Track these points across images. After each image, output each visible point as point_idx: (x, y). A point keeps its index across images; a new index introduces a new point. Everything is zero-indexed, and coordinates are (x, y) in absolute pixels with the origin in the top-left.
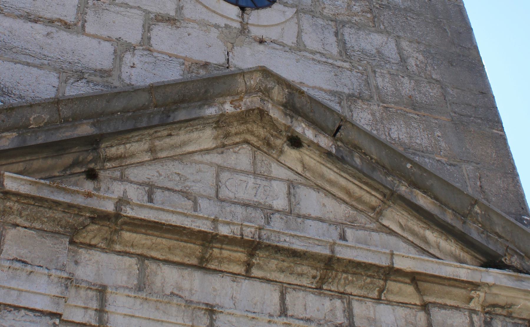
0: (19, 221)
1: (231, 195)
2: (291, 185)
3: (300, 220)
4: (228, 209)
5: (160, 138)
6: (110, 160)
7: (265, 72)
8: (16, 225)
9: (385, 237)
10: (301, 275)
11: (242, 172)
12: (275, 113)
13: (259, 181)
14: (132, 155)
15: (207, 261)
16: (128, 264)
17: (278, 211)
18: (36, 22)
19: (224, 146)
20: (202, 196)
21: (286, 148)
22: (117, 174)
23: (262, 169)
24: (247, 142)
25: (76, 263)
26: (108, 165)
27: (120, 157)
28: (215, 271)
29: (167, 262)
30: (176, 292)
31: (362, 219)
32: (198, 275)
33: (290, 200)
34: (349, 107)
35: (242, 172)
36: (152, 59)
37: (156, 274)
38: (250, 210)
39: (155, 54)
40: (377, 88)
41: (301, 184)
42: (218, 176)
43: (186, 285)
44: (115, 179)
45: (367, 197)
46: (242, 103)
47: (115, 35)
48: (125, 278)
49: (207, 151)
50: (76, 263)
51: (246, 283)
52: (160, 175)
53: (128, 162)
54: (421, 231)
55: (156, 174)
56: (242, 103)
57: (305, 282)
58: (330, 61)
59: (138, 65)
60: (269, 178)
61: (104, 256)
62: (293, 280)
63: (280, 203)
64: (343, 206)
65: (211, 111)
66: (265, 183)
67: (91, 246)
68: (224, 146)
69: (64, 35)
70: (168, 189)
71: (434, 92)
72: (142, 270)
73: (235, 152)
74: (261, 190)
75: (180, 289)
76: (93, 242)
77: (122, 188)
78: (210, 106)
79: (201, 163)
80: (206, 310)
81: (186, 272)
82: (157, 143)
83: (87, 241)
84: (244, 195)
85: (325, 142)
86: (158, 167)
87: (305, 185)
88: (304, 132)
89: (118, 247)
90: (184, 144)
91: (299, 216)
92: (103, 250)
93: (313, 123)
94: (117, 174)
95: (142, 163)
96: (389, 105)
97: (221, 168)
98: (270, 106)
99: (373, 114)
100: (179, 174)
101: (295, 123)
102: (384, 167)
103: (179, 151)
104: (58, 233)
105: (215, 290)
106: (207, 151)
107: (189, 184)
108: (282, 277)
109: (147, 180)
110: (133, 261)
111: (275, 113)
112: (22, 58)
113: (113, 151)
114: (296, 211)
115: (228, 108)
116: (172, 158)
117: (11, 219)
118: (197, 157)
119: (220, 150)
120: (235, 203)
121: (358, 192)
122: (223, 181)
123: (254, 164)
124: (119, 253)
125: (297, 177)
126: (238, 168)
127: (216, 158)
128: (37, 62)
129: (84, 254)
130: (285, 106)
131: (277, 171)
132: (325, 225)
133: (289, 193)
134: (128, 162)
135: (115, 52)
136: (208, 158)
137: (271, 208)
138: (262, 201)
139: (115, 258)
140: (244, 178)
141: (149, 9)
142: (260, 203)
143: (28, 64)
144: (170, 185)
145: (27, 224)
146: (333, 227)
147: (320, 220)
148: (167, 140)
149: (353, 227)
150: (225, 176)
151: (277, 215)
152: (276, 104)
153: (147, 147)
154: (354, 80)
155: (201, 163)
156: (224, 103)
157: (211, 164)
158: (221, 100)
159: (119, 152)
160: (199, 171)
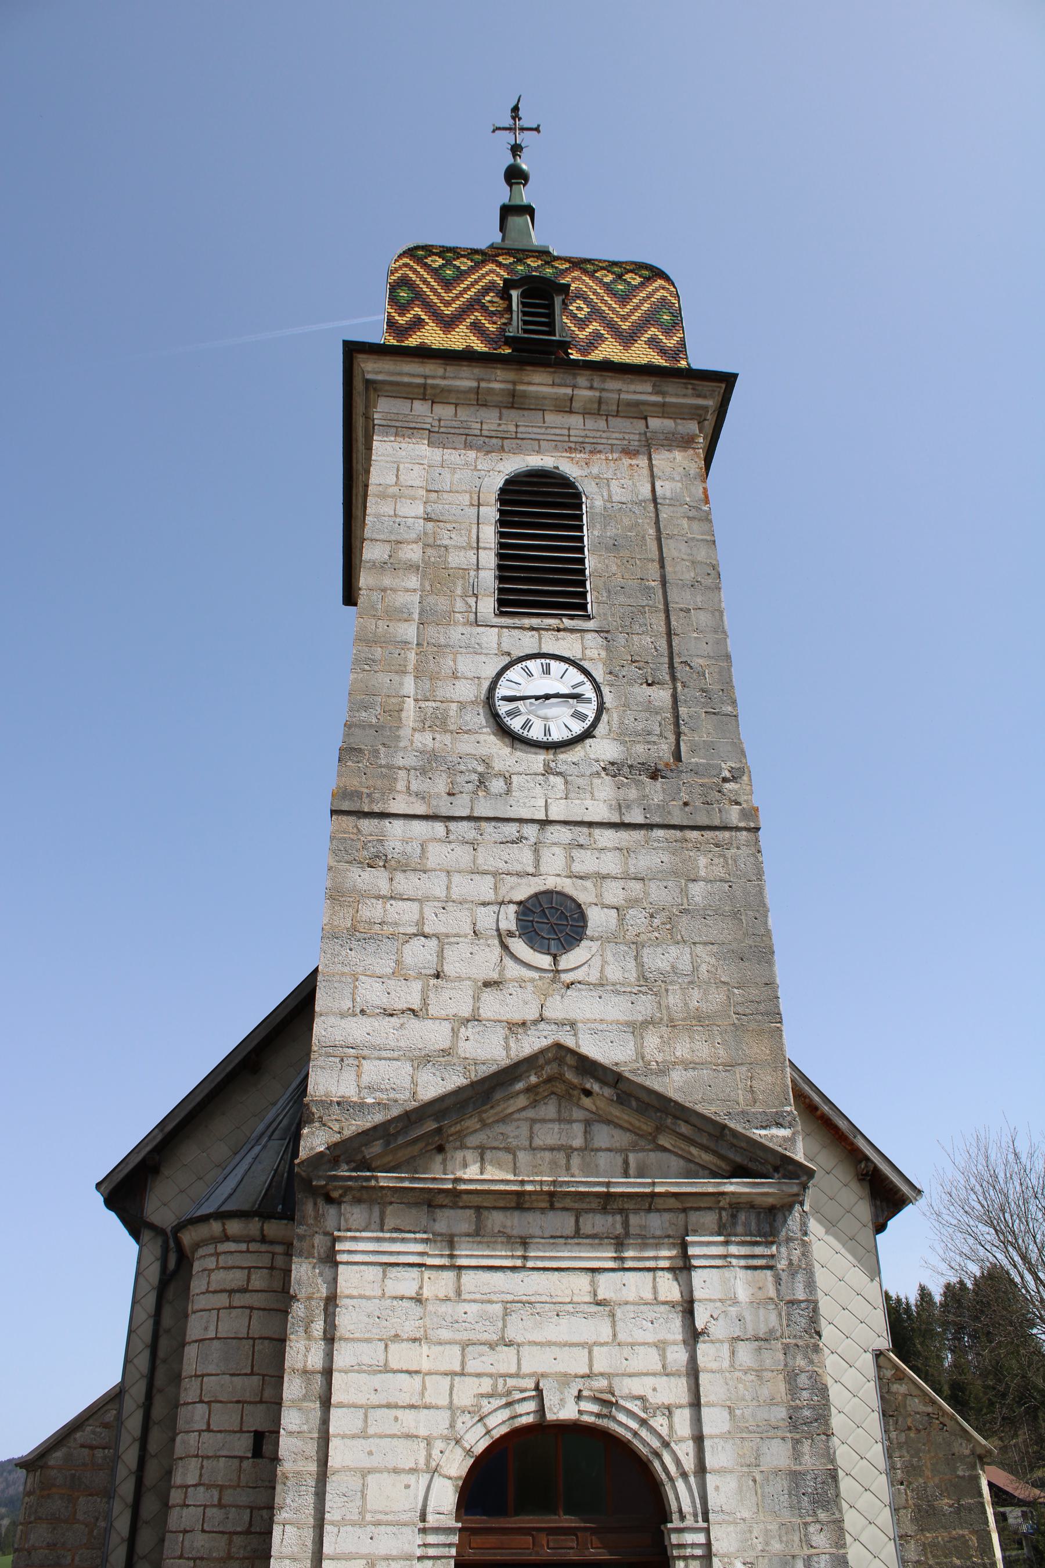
0: (393, 1199)
1: (541, 1143)
2: (588, 1123)
3: (593, 1153)
4: (539, 1156)
5: (486, 1111)
6: (451, 1135)
7: (558, 1046)
8: (391, 1203)
9: (660, 1155)
10: (590, 1202)
11: (550, 1121)
12: (570, 1076)
13: (562, 1126)
14: (468, 1128)
15: (522, 1204)
16: (468, 1214)
17: (576, 1149)
18: (392, 1015)
19: (536, 1101)
20: (520, 1149)
21: (582, 1096)
22: (458, 1143)
23: (565, 1115)
24: (553, 1093)
25: (434, 1220)
26: (451, 1138)
27: (459, 1132)
28: (529, 1209)
29: (495, 1208)
30: (502, 1230)
31: (642, 1143)
32: (516, 1214)
33: (586, 1138)
34: (641, 1035)
35: (550, 1121)
36: (481, 1028)
37: (488, 1218)
38: (555, 1153)
39: (484, 1022)
40: (668, 1007)
41: (595, 1121)
42: (531, 1128)
43: (509, 1223)
44: (456, 1149)
45: (644, 1127)
46: (544, 1072)
47: (451, 1012)
48: (467, 1226)
49: (524, 1109)
50: (434, 1220)
51: (551, 1214)
52: (489, 1137)
53: (465, 1133)
54: (687, 1148)
55: (486, 1137)
56: (544, 1072)
57: (594, 1206)
58: (628, 989)
59: (471, 1038)
60: (570, 1122)
61: (452, 1211)
62: (585, 1206)
63: (578, 1142)
64: (628, 1134)
65: (520, 1086)
66: (567, 1126)
67: (442, 1206)
68: (536, 1101)
69: (413, 1023)
70: (495, 1148)
71: (718, 997)
72: (478, 1217)
73: (545, 1104)
74: (564, 1133)
75: (505, 1227)
76: (444, 1203)
77: (462, 1154)
78: (519, 1081)
79: (519, 1120)
80: (521, 1242)
81: (508, 1213)
82: (484, 1116)
83: (440, 1203)
84: (550, 1141)
85: (608, 1092)
86: (488, 1132)
87: (598, 1121)
88: (592, 1087)
89: (461, 1204)
90: (505, 1109)
91: (592, 1150)
92: (451, 1208)
93: (598, 1079)
94: (458, 1143)
95: (475, 1131)
96: (677, 1023)
97: (534, 1121)
98: (566, 1069)
99: (661, 1037)
100: (502, 1134)
101: (585, 1081)
102: (653, 1107)
103: (502, 1115)
104: (420, 1203)
105: (529, 1223)
106: (524, 1109)
107: (510, 1140)
108: (576, 1206)
109: (479, 1144)
110: (472, 1211)
111: (570, 1076)
112: (384, 1054)
113: (453, 1130)
114: (591, 1146)
115: (533, 1079)
116: (497, 1121)
117: (389, 1199)
118: (516, 1116)
119: (533, 1105)
120: (544, 1149)
121: (637, 1124)
122: (535, 1132)
123: (559, 1111)
124: (462, 1208)
125: (592, 1116)
126: (547, 1118)
127: (530, 1113)
128: (396, 1054)
129: (439, 1213)
130: (576, 1068)
131: (577, 1114)
132: (612, 1154)
133: (586, 1132)
134: (465, 1133)
135: (453, 1029)
136: (524, 1114)
137: (571, 1147)
138: (564, 1143)
139: (460, 1211)
140: (550, 1126)
141: (475, 976)
142: (563, 1145)
143: (390, 1059)
144: (496, 1144)
145: (399, 1201)
146: (619, 1154)
147: (609, 1150)
148: (491, 1111)
149: (634, 1151)
150: (537, 1126)
151: (576, 1153)
152: (570, 1067)
153: (476, 1120)
154: (648, 1005)
155: (519, 1120)
156: (528, 1077)
157: (526, 1119)
158: (527, 1074)
159: (457, 1129)
160: (518, 1127)
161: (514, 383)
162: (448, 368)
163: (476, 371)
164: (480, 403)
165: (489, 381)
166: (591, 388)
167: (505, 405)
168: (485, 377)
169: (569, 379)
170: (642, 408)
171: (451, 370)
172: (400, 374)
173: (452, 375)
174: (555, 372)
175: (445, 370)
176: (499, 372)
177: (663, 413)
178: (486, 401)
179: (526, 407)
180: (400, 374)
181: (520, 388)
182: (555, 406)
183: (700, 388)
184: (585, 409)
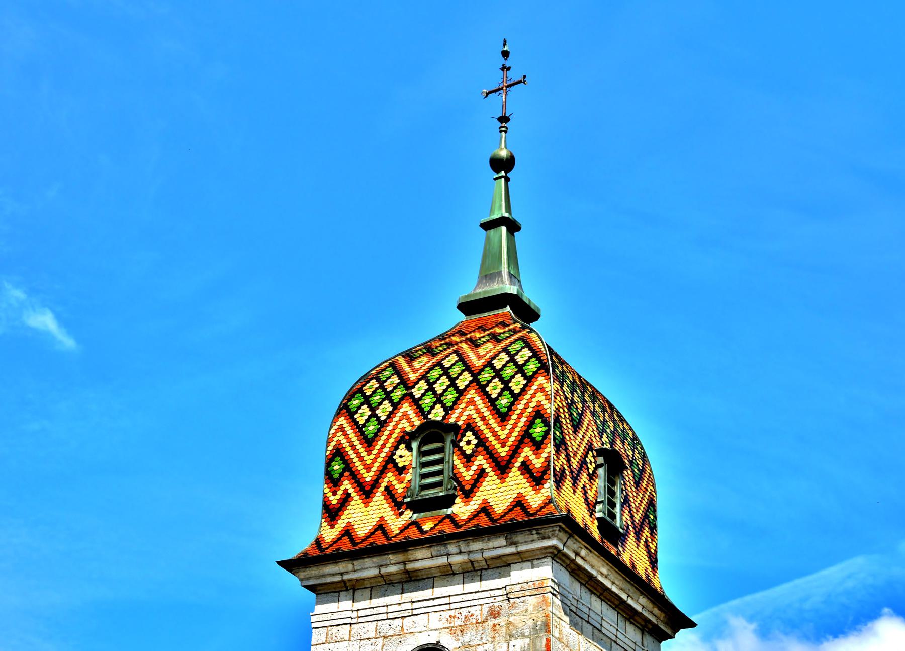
161: (404, 563)
162: (355, 563)
163: (375, 560)
164: (387, 582)
165: (386, 565)
166: (461, 553)
167: (405, 580)
168: (383, 563)
169: (442, 550)
170: (504, 559)
171: (358, 564)
172: (324, 576)
173: (359, 568)
174: (431, 547)
175: (353, 564)
176: (391, 557)
177: (522, 559)
178: (391, 580)
179: (421, 577)
180: (324, 576)
181: (410, 566)
182: (441, 572)
183: (542, 531)
184: (463, 569)
